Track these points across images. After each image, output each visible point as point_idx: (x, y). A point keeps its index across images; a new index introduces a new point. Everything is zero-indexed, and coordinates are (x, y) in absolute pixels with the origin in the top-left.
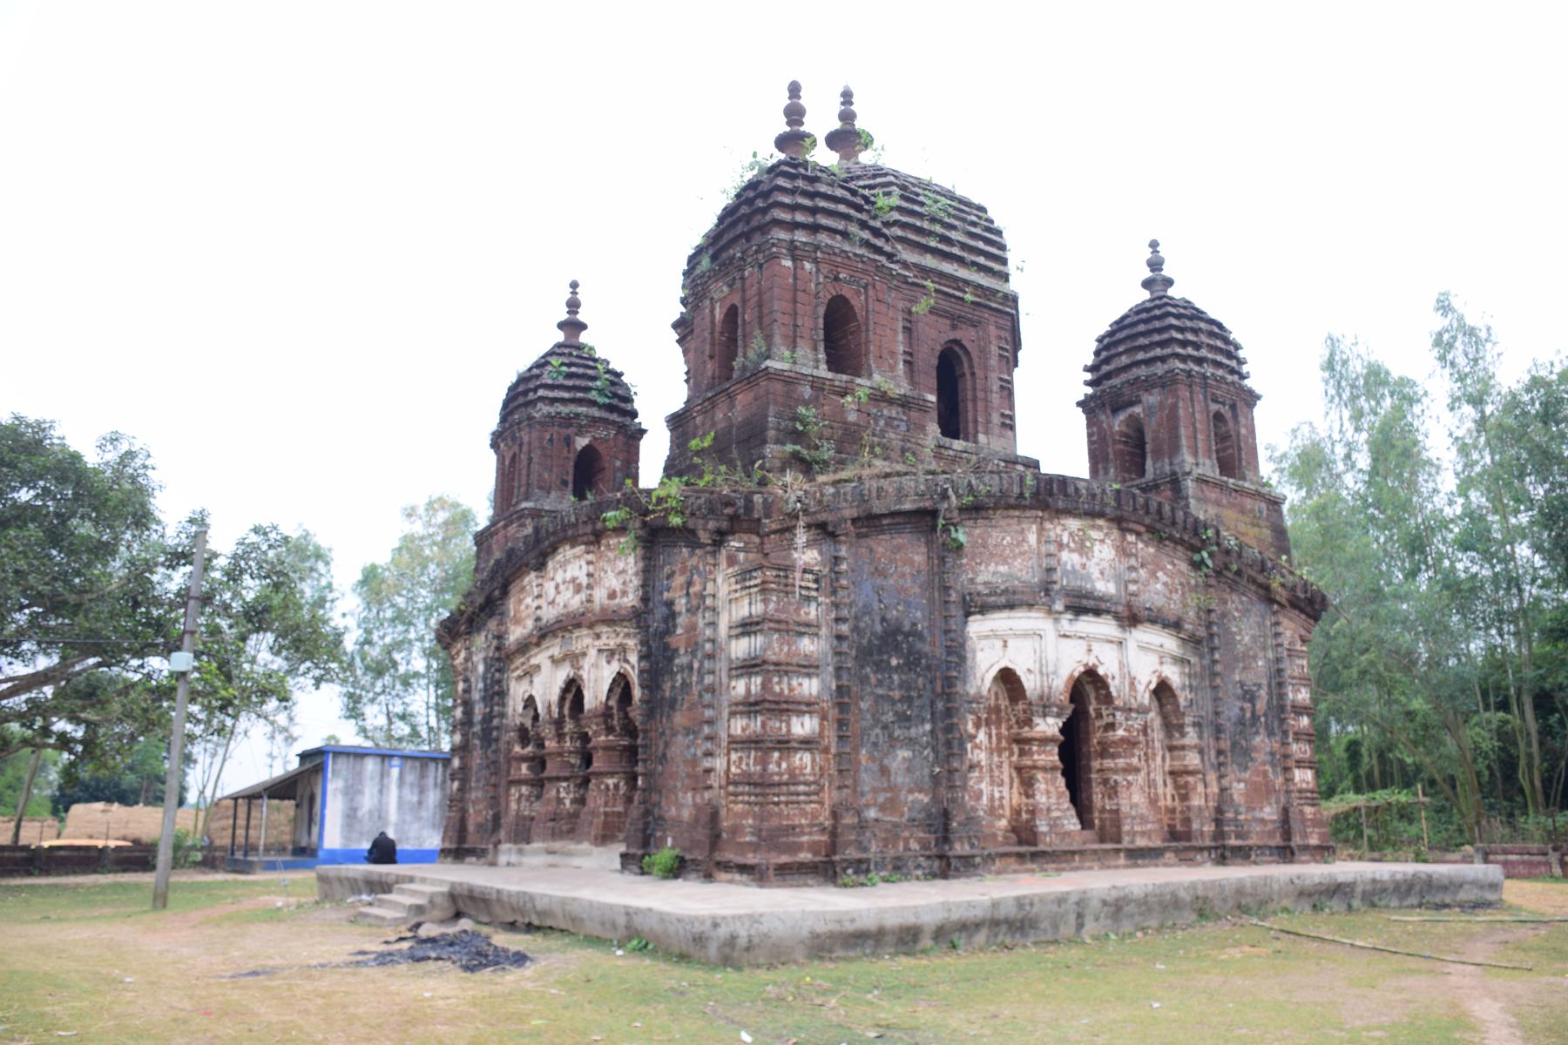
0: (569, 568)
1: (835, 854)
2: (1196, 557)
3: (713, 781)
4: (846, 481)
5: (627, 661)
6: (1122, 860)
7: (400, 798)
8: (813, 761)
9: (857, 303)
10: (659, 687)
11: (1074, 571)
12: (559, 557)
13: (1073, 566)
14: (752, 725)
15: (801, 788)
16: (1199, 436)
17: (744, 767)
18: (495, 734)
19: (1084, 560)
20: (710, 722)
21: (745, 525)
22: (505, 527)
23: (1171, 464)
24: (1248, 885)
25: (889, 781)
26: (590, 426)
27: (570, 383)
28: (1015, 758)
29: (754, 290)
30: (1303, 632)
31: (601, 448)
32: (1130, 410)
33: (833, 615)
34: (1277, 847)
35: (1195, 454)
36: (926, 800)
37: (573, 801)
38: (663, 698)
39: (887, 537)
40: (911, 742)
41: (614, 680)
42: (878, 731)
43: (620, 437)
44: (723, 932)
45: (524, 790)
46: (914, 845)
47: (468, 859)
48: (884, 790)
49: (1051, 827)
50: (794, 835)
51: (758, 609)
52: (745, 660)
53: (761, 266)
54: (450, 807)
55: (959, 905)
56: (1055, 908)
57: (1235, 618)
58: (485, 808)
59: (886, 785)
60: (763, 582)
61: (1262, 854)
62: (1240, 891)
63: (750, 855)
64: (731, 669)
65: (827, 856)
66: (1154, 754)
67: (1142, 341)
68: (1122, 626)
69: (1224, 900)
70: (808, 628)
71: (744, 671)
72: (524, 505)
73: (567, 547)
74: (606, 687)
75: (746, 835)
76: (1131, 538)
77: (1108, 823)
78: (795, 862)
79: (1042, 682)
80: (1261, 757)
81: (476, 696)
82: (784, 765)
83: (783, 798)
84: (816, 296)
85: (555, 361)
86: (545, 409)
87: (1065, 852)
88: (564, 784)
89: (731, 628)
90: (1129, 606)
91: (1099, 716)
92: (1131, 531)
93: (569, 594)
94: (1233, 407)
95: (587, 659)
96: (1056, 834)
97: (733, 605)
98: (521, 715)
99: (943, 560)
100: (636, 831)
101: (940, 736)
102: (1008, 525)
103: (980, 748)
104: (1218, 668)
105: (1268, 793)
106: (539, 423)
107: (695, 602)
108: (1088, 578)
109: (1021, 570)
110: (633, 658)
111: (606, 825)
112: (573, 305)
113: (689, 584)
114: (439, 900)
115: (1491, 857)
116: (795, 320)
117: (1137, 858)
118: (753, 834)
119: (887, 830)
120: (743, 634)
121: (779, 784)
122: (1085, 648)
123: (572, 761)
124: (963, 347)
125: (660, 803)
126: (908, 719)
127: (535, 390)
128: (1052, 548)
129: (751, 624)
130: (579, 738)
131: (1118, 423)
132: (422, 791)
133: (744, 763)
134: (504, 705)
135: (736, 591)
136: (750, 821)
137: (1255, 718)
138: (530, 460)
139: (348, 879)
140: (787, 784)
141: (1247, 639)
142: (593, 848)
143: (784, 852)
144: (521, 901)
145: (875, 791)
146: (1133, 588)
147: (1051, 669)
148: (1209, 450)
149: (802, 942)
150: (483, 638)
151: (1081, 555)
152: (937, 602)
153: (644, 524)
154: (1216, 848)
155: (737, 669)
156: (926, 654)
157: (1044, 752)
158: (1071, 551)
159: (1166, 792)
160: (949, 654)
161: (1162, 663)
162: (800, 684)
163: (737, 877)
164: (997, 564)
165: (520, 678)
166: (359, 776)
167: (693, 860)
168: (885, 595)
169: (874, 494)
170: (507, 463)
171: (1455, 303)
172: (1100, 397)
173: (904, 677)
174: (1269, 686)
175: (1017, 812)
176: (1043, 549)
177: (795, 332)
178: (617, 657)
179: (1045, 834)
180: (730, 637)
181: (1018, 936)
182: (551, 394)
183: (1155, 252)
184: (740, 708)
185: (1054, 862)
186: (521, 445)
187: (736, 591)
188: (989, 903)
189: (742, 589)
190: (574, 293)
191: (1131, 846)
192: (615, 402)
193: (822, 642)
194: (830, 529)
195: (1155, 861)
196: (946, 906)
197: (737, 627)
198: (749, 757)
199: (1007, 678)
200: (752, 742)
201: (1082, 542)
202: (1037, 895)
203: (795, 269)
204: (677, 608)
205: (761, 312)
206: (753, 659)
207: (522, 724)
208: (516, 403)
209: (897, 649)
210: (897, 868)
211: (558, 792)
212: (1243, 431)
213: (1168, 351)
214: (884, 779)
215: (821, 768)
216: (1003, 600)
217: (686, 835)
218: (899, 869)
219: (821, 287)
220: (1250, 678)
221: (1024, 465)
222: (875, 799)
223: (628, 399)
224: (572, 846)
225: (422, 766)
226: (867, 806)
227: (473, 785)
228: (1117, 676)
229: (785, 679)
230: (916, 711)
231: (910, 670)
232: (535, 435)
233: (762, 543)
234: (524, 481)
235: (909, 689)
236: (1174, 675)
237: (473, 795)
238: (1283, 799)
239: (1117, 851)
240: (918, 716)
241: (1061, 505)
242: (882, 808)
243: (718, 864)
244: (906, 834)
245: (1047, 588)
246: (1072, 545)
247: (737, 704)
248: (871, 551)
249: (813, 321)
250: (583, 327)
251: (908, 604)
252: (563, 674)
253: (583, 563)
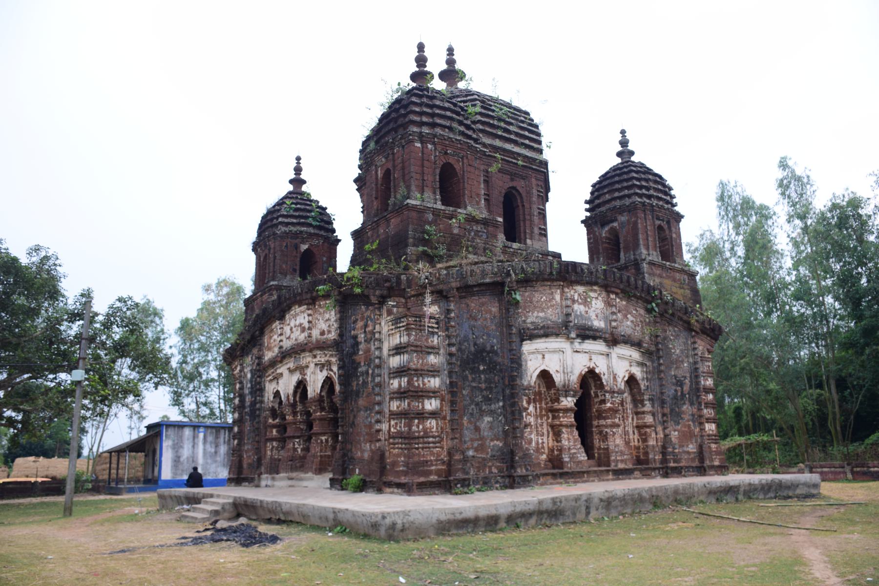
0: (298, 318)
1: (450, 476)
2: (649, 306)
3: (381, 436)
4: (453, 267)
5: (332, 370)
6: (611, 477)
7: (204, 450)
8: (437, 424)
9: (458, 167)
10: (350, 384)
11: (581, 315)
12: (292, 312)
13: (580, 312)
14: (403, 405)
15: (431, 439)
16: (650, 239)
17: (398, 428)
18: (258, 412)
19: (587, 309)
20: (379, 403)
21: (396, 293)
22: (261, 295)
23: (634, 255)
24: (681, 488)
25: (480, 434)
26: (309, 238)
27: (297, 214)
28: (550, 421)
29: (399, 160)
30: (709, 347)
31: (315, 250)
32: (611, 225)
33: (447, 342)
34: (697, 467)
35: (648, 249)
36: (501, 445)
37: (301, 451)
38: (352, 391)
39: (477, 298)
40: (491, 413)
41: (324, 381)
42: (473, 406)
43: (326, 244)
44: (388, 521)
45: (275, 444)
46: (495, 470)
47: (244, 484)
48: (477, 440)
49: (571, 458)
50: (427, 466)
51: (405, 339)
53: (403, 147)
54: (233, 454)
55: (520, 503)
56: (573, 503)
57: (671, 340)
58: (253, 455)
59: (478, 437)
60: (407, 324)
61: (689, 471)
62: (676, 491)
63: (403, 478)
64: (390, 374)
65: (446, 477)
66: (628, 417)
67: (617, 186)
68: (608, 346)
69: (668, 497)
70: (434, 350)
71: (397, 374)
72: (272, 283)
73: (297, 307)
74: (320, 385)
76: (613, 296)
77: (602, 455)
78: (428, 481)
79: (564, 377)
80: (686, 417)
81: (247, 391)
82: (421, 427)
83: (420, 445)
84: (435, 163)
85: (288, 202)
86: (284, 229)
87: (579, 472)
88: (297, 440)
89: (389, 350)
90: (612, 334)
91: (597, 396)
92: (613, 292)
93: (298, 333)
94: (668, 222)
95: (309, 369)
96: (574, 462)
97: (391, 338)
98: (272, 402)
99: (508, 310)
100: (338, 466)
101: (508, 409)
102: (544, 290)
103: (531, 415)
104: (662, 368)
105: (691, 437)
106: (280, 236)
107: (369, 336)
108: (589, 319)
109: (552, 315)
110: (335, 368)
111: (321, 463)
112: (298, 170)
113: (366, 326)
114: (227, 507)
115: (814, 470)
116: (423, 177)
117: (619, 475)
118: (404, 466)
119: (479, 462)
120: (397, 354)
121: (418, 438)
122: (588, 358)
123: (302, 427)
124: (517, 191)
126: (490, 399)
127: (277, 218)
128: (569, 303)
129: (401, 348)
130: (305, 414)
131: (604, 232)
132: (217, 446)
133: (399, 426)
134: (262, 396)
135: (392, 330)
136: (402, 459)
137: (683, 395)
138: (275, 257)
139: (176, 496)
140: (423, 437)
141: (678, 351)
143: (422, 476)
144: (274, 508)
145: (472, 440)
146: (614, 324)
147: (569, 370)
148: (655, 246)
149: (433, 526)
150: (250, 359)
151: (585, 306)
152: (505, 334)
153: (340, 293)
154: (662, 468)
155: (393, 373)
156: (499, 364)
157: (566, 417)
158: (580, 304)
159: (634, 438)
160: (512, 363)
161: (631, 366)
162: (429, 381)
163: (396, 490)
164: (538, 312)
165: (271, 381)
166: (181, 438)
167: (370, 481)
168: (476, 330)
169: (469, 274)
170: (262, 259)
171: (790, 163)
172: (594, 218)
173: (487, 376)
174: (691, 377)
175: (551, 450)
176: (564, 303)
177: (423, 183)
178: (326, 368)
179: (567, 462)
180: (389, 355)
181: (553, 519)
182: (286, 220)
183: (624, 136)
184: (396, 395)
185: (573, 478)
186: (269, 250)
187: (392, 330)
188: (537, 502)
189: (395, 328)
190: (298, 163)
191: (616, 468)
192: (322, 224)
193: (441, 357)
194: (445, 294)
195: (629, 476)
196: (513, 504)
197: (393, 350)
198: (401, 423)
199: (545, 376)
200: (402, 414)
201: (586, 298)
202: (564, 496)
203: (423, 148)
204: (359, 340)
205: (404, 173)
206: (402, 367)
207: (273, 407)
208: (266, 226)
209: (483, 361)
210: (485, 483)
211: (294, 444)
212: (674, 236)
213: (632, 191)
214: (477, 433)
215: (442, 428)
216: (542, 332)
217: (366, 467)
218: (486, 484)
219: (437, 158)
220: (680, 373)
221: (553, 256)
222: (472, 445)
223: (330, 223)
224: (302, 475)
225: (216, 431)
226: (468, 449)
228: (606, 373)
229: (421, 379)
230: (494, 395)
231: (490, 372)
232: (277, 243)
233: (406, 303)
234: (271, 268)
235: (490, 383)
236: (638, 372)
237: (246, 448)
238: (699, 440)
239: (608, 471)
240: (495, 398)
241: (573, 278)
242: (476, 450)
243: (385, 483)
244: (490, 464)
245: (566, 324)
246: (580, 301)
247: (393, 393)
248: (468, 305)
249: (433, 177)
250: (304, 182)
251: (489, 335)
252: (296, 377)
253: (306, 315)
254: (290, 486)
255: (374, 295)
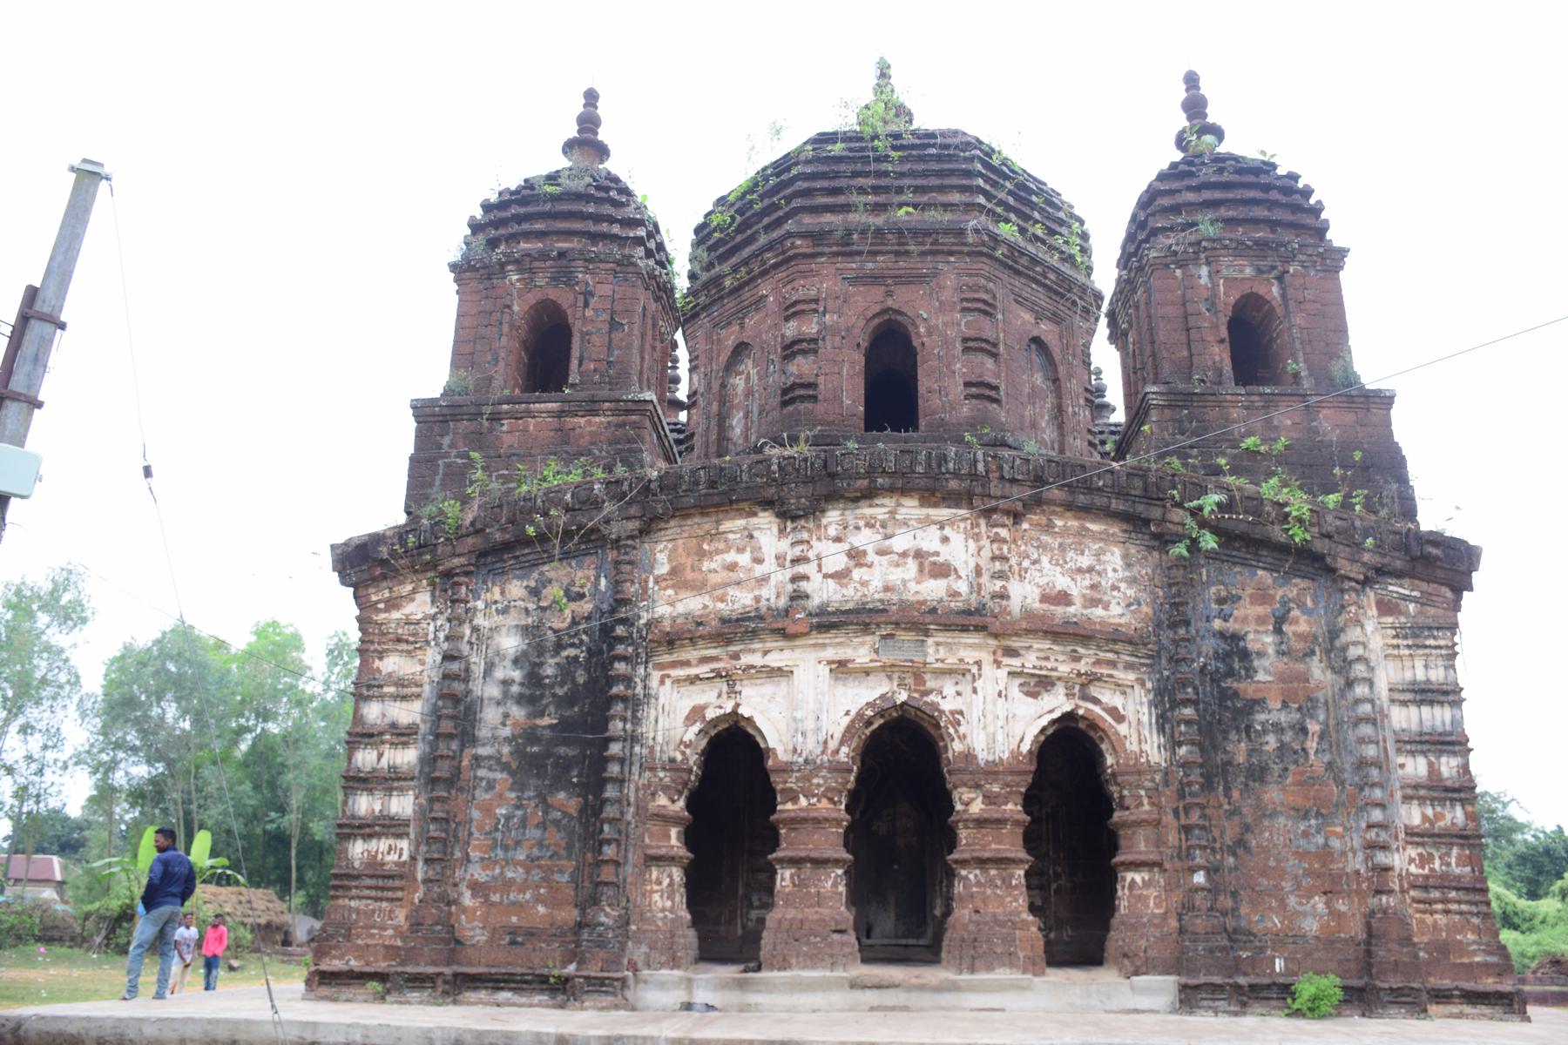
14: (1449, 816)
17: (1437, 864)
18: (614, 769)
38: (1229, 763)
47: (471, 995)
52: (1421, 734)
63: (1490, 980)
75: (1474, 953)
89: (1390, 690)
100: (1212, 952)
125: (1235, 910)
129: (1432, 691)
134: (636, 721)
142: (1029, 976)
163: (1468, 1009)
165: (693, 680)
178: (1060, 689)
184: (1422, 792)
187: (1398, 646)
189: (1409, 647)
197: (1403, 691)
198: (1448, 854)
204: (1252, 644)
206: (1440, 734)
227: (475, 855)
247: (1416, 787)
254: (872, 1009)
255: (1353, 561)
